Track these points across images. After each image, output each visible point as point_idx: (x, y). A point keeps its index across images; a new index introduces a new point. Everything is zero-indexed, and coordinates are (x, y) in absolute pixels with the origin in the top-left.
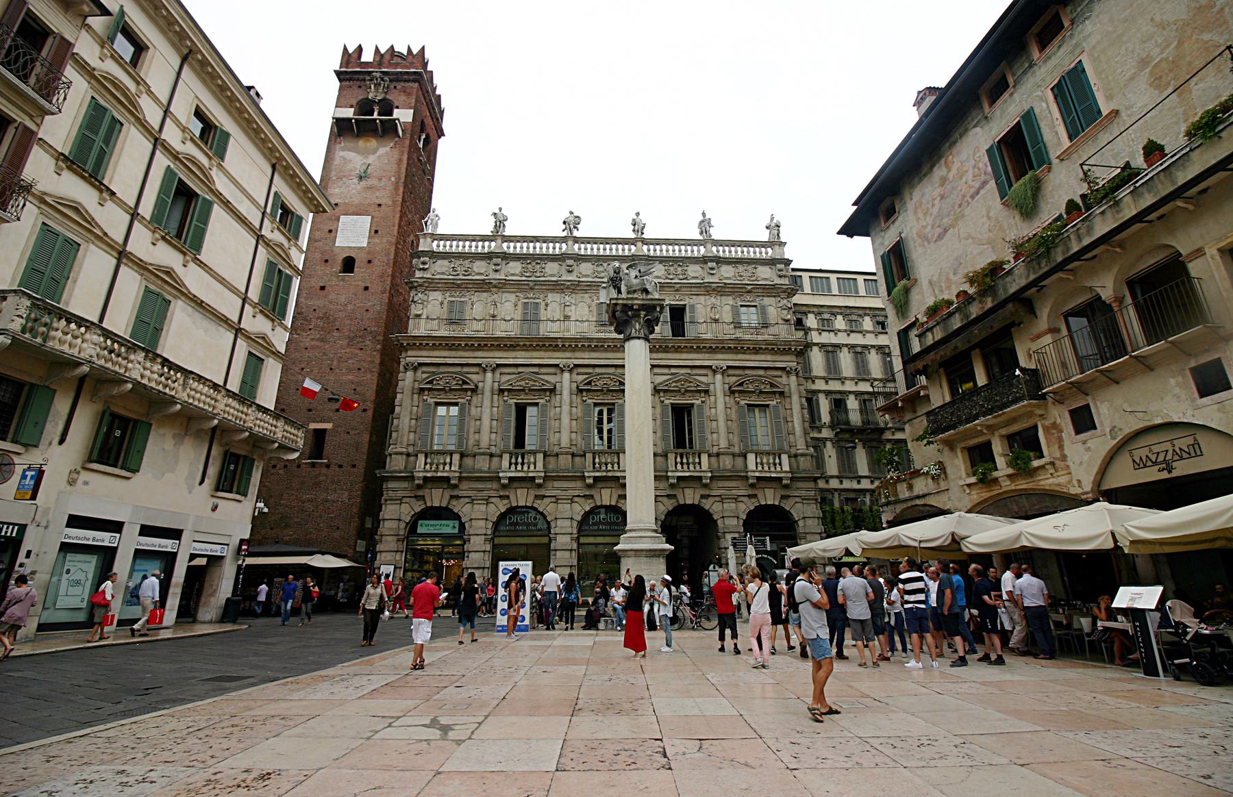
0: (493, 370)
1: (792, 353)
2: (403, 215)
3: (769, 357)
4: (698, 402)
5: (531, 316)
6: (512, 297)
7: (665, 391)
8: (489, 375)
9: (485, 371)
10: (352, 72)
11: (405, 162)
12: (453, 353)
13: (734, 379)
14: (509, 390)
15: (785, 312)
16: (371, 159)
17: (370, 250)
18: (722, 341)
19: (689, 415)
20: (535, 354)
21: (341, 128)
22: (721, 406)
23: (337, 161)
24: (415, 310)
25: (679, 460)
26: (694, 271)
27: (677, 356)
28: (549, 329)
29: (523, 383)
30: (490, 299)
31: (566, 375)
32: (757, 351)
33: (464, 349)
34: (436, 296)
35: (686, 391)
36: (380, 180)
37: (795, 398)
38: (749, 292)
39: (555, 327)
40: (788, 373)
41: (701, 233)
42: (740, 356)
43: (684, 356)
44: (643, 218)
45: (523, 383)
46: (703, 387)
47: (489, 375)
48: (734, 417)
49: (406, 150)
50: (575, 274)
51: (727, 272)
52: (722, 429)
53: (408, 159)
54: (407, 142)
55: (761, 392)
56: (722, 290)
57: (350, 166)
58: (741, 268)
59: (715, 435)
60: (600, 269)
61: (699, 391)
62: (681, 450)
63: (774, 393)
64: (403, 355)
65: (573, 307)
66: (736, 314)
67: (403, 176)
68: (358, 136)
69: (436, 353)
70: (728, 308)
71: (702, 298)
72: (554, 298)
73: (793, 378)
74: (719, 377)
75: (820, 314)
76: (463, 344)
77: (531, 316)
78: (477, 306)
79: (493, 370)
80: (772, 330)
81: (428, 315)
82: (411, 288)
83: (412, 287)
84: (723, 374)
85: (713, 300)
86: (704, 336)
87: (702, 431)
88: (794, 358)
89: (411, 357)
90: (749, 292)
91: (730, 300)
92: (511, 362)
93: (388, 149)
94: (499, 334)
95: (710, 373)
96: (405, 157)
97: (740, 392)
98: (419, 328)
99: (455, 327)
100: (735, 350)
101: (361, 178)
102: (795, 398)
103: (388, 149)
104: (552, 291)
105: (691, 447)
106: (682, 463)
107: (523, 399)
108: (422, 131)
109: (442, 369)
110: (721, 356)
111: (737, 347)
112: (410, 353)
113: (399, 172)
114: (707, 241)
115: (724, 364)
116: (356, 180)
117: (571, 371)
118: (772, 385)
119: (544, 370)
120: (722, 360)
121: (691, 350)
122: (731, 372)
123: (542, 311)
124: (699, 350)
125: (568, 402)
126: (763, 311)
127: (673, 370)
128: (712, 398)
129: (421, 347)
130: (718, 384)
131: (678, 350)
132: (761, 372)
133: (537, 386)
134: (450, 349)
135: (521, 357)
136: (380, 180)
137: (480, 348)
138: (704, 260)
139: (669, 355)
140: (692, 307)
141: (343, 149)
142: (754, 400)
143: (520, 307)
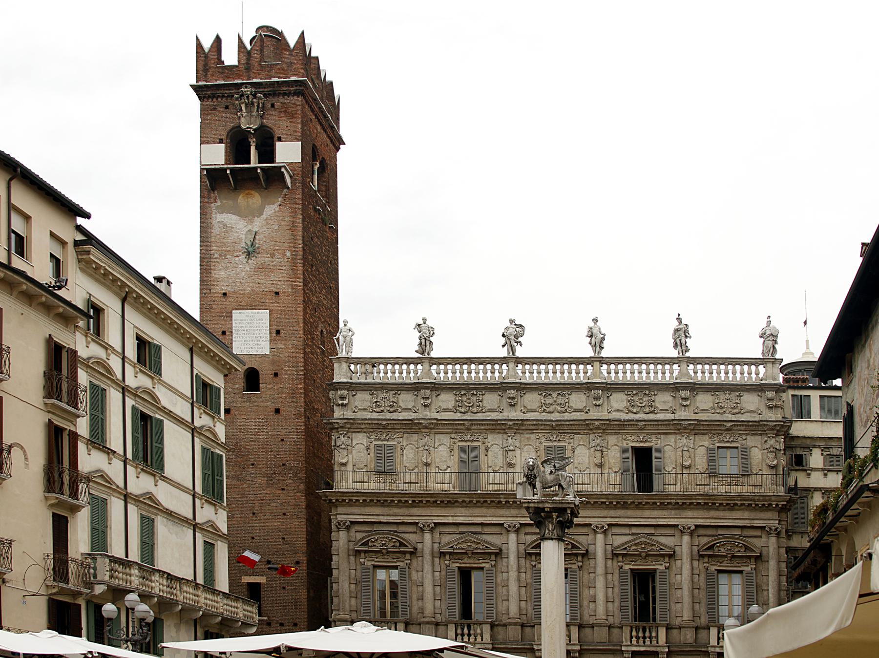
0: (432, 530)
1: (774, 509)
2: (306, 302)
3: (746, 514)
4: (661, 568)
5: (470, 465)
6: (446, 440)
7: (624, 555)
8: (428, 536)
9: (422, 530)
10: (216, 85)
11: (300, 226)
12: (386, 510)
13: (704, 540)
14: (450, 553)
15: (771, 456)
16: (257, 224)
17: (273, 359)
18: (690, 497)
19: (654, 582)
20: (477, 511)
21: (213, 181)
22: (686, 571)
23: (216, 230)
24: (340, 457)
25: (634, 633)
26: (663, 400)
27: (638, 513)
28: (491, 481)
29: (464, 546)
30: (421, 443)
31: (513, 537)
32: (732, 507)
33: (397, 506)
34: (360, 440)
35: (648, 555)
36: (272, 255)
37: (772, 564)
38: (729, 430)
39: (499, 478)
40: (769, 533)
41: (675, 346)
42: (713, 513)
43: (647, 513)
44: (604, 326)
45: (464, 546)
46: (668, 551)
47: (428, 536)
48: (703, 584)
49: (299, 207)
50: (518, 408)
51: (704, 401)
52: (687, 599)
53: (304, 220)
54: (299, 195)
55: (733, 557)
56: (695, 428)
57: (233, 236)
58: (722, 396)
59: (679, 605)
60: (549, 400)
61: (663, 556)
62: (644, 624)
63: (749, 557)
64: (333, 511)
65: (518, 452)
66: (712, 455)
67: (300, 247)
68: (236, 189)
69: (368, 510)
70: (702, 451)
71: (672, 438)
72: (495, 440)
73: (773, 540)
74: (686, 539)
75: (828, 448)
76: (396, 500)
77: (470, 465)
78: (408, 452)
79: (432, 530)
80: (754, 480)
81: (354, 464)
82: (331, 429)
83: (333, 428)
84: (691, 534)
85: (684, 440)
86: (671, 489)
87: (664, 601)
88: (775, 515)
89: (342, 515)
90: (729, 430)
91: (705, 441)
92: (450, 520)
93: (275, 207)
94: (436, 487)
95: (677, 533)
96: (299, 219)
97: (709, 556)
98: (347, 482)
99: (385, 477)
100: (705, 506)
101: (249, 254)
102: (772, 564)
103: (275, 207)
104: (493, 431)
105: (654, 620)
106: (637, 638)
107: (466, 563)
108: (314, 158)
109: (376, 528)
110: (689, 513)
111: (708, 503)
112: (340, 510)
113: (294, 242)
114: (684, 360)
115: (692, 523)
116: (242, 257)
117: (517, 531)
118: (747, 548)
119: (487, 530)
120: (690, 519)
121: (653, 506)
122: (702, 531)
123: (482, 456)
124: (663, 506)
125: (515, 567)
126: (745, 454)
127: (634, 530)
128: (678, 563)
129: (351, 503)
130: (685, 546)
131: (639, 506)
132: (737, 532)
133: (481, 549)
134: (383, 506)
135: (461, 516)
136: (272, 255)
137: (414, 504)
138: (674, 388)
139: (629, 513)
140: (659, 450)
141: (222, 210)
142: (726, 565)
143: (456, 452)
